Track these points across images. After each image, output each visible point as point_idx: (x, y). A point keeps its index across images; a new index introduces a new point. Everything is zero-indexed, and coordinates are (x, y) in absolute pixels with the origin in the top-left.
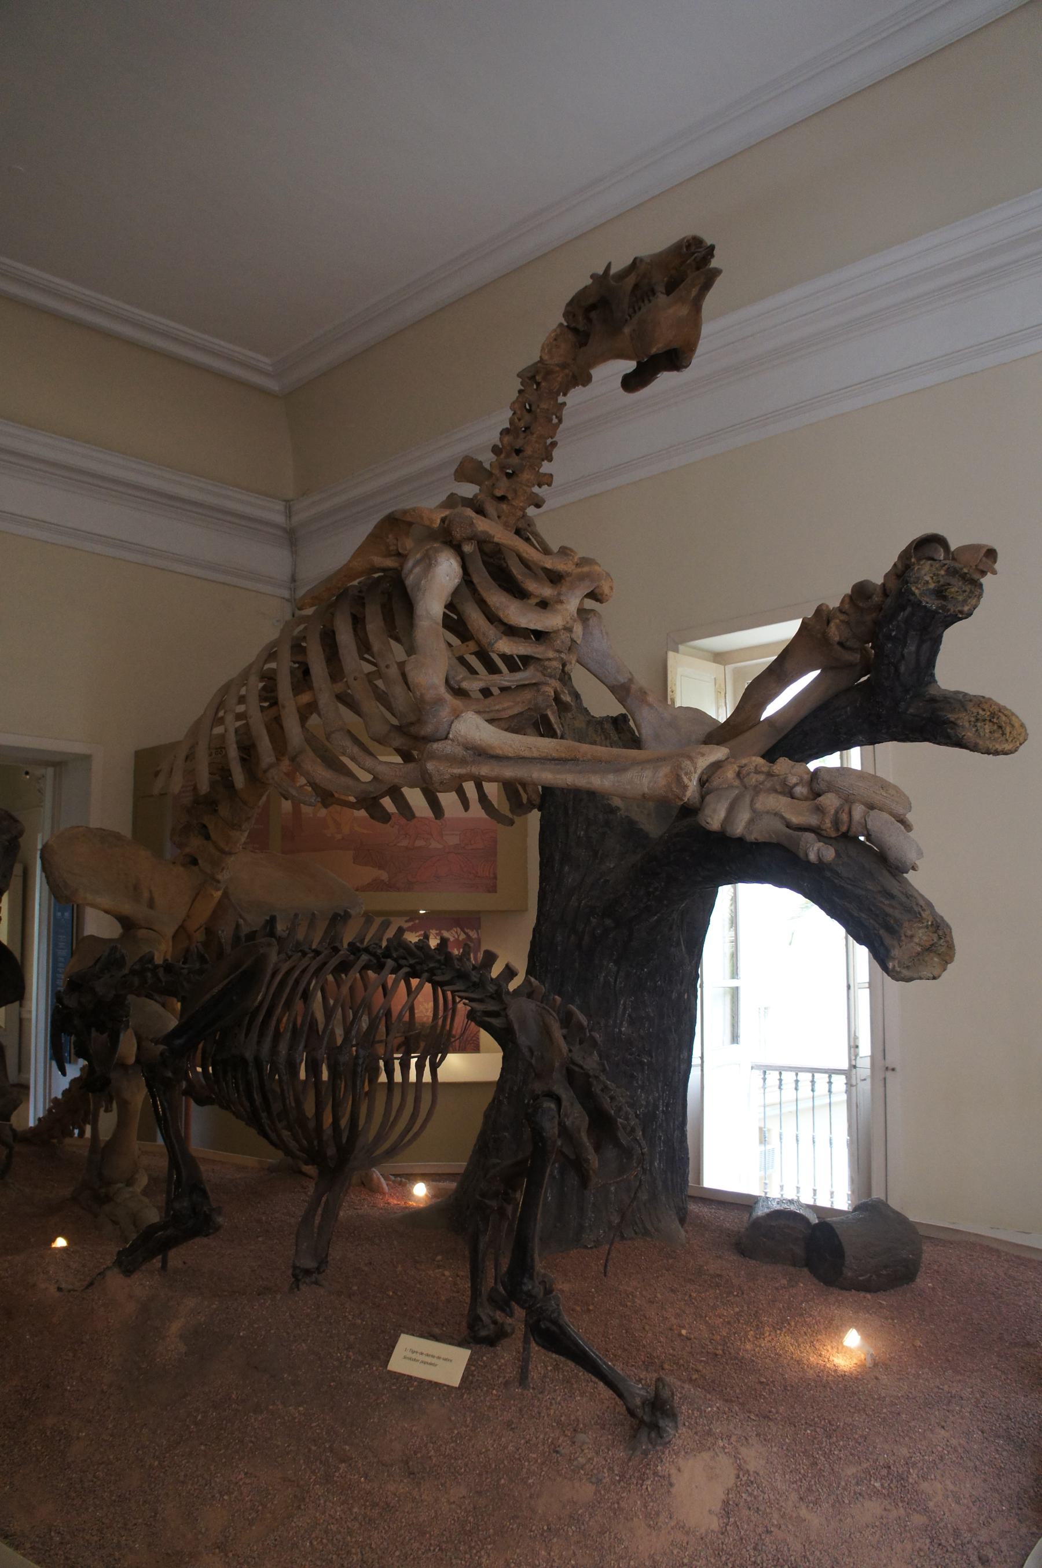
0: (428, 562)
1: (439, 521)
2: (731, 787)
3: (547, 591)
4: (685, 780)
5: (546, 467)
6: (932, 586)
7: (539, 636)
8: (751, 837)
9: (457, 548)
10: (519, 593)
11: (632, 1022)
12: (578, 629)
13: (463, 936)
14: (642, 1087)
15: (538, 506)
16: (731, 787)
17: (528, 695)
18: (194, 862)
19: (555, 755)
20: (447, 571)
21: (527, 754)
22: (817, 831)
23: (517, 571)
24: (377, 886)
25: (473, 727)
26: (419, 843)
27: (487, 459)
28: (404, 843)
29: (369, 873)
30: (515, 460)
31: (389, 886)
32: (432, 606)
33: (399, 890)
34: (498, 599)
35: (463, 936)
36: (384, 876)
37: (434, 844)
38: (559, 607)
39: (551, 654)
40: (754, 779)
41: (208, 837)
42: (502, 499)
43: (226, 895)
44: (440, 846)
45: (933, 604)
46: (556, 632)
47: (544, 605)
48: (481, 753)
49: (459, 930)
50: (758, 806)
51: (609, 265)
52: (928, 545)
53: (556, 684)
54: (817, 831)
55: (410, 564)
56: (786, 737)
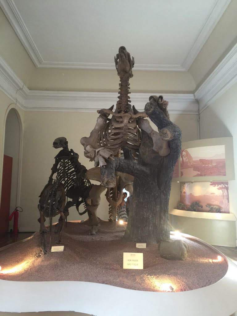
3: (121, 120)
10: (118, 122)
13: (224, 186)
14: (146, 212)
15: (130, 102)
24: (198, 175)
26: (206, 166)
28: (203, 166)
29: (196, 173)
31: (201, 175)
33: (203, 176)
35: (224, 186)
36: (199, 173)
37: (210, 166)
39: (123, 131)
43: (120, 177)
44: (211, 166)
46: (123, 127)
49: (223, 185)
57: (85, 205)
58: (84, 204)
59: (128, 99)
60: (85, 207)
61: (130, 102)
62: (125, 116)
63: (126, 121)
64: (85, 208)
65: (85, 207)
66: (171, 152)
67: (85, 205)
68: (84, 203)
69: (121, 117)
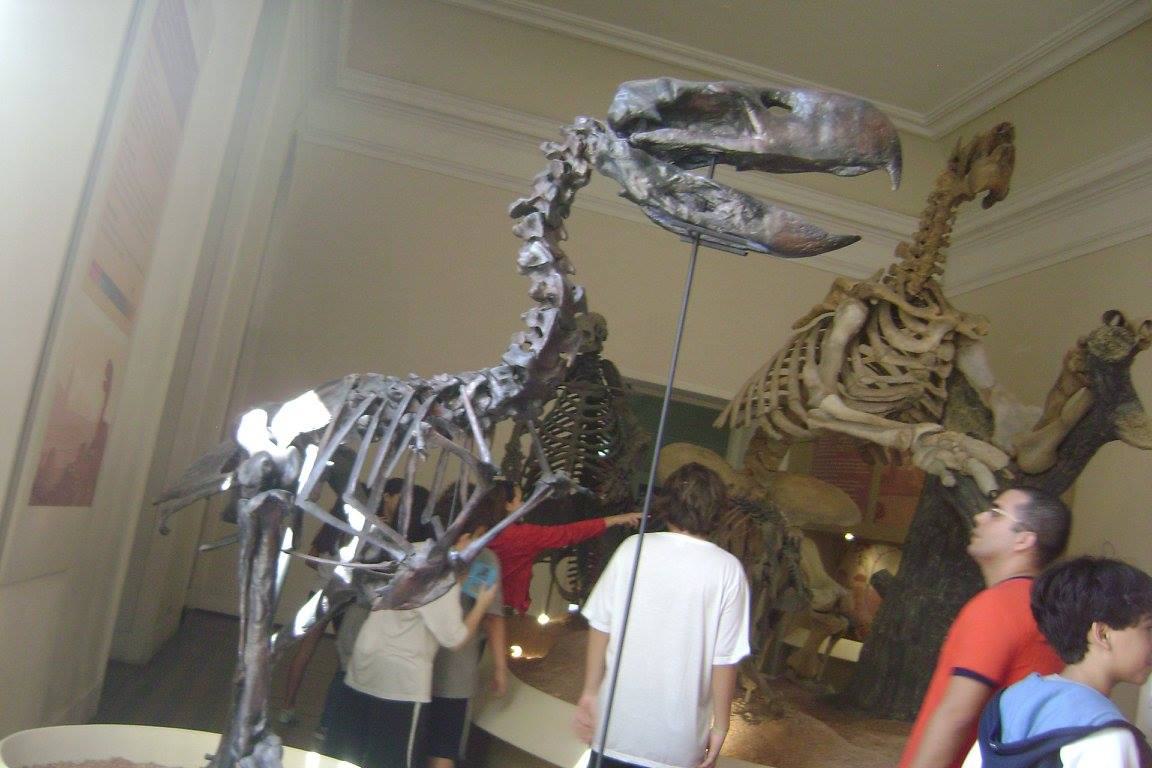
0: (843, 309)
1: (852, 287)
2: (931, 446)
3: (921, 328)
4: (903, 439)
5: (942, 250)
6: (1103, 342)
7: (916, 355)
8: (930, 472)
9: (866, 301)
11: (946, 594)
12: (947, 352)
16: (931, 446)
17: (904, 389)
18: (752, 474)
19: (866, 421)
20: (852, 316)
21: (852, 419)
22: (954, 471)
23: (902, 317)
25: (832, 403)
27: (912, 242)
30: (921, 247)
32: (840, 334)
34: (890, 332)
38: (928, 339)
39: (919, 366)
40: (945, 442)
41: (760, 460)
42: (911, 270)
45: (1097, 353)
47: (919, 337)
48: (834, 418)
50: (938, 456)
51: (960, 139)
52: (1109, 316)
53: (930, 386)
54: (954, 471)
55: (837, 309)
56: (1073, 430)
57: (574, 565)
58: (570, 562)
59: (937, 264)
60: (575, 572)
61: (941, 272)
62: (941, 322)
63: (935, 336)
64: (570, 576)
65: (575, 572)
66: (1056, 465)
67: (574, 565)
68: (574, 558)
69: (925, 321)
